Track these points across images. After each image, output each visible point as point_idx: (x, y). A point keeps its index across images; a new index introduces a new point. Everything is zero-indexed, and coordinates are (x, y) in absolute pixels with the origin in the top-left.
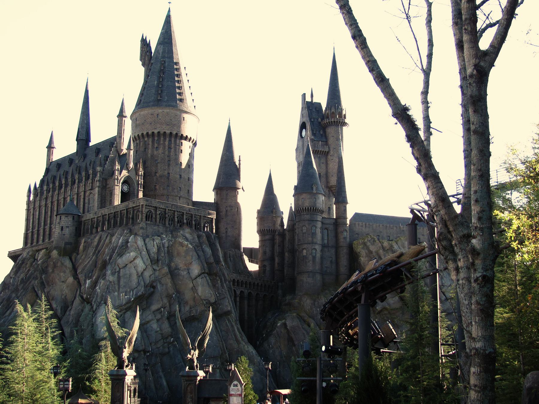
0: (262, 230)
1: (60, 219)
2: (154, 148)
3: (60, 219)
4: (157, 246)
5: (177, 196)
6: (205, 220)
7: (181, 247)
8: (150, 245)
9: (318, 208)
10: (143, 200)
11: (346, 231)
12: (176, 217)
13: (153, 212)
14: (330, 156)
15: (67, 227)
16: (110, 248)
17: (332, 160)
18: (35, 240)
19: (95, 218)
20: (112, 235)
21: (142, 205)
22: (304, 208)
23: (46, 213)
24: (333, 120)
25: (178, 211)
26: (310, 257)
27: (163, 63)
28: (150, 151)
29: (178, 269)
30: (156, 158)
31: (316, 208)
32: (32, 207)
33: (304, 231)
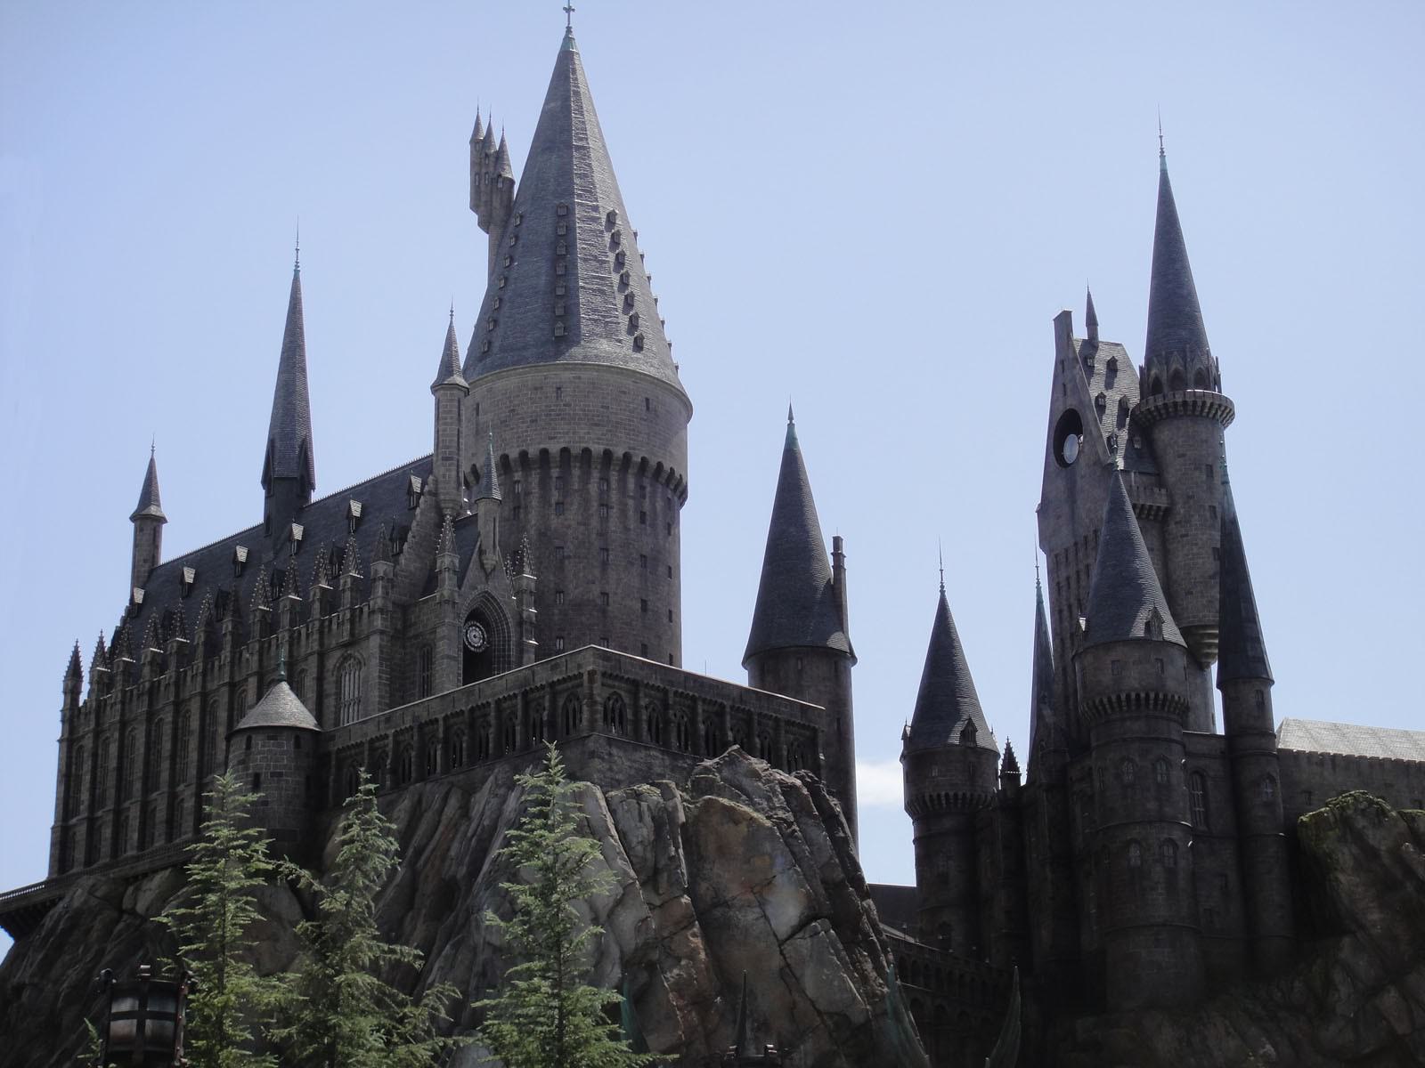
0: (927, 798)
1: (249, 747)
2: (550, 506)
3: (249, 747)
4: (653, 818)
6: (792, 737)
7: (731, 825)
8: (628, 815)
9: (1173, 696)
10: (594, 654)
11: (1273, 780)
12: (700, 719)
13: (627, 701)
14: (1176, 523)
15: (273, 774)
16: (469, 834)
17: (1182, 536)
18: (105, 848)
19: (386, 736)
20: (469, 791)
21: (592, 674)
22: (1123, 697)
23: (152, 745)
24: (1179, 399)
25: (704, 701)
26: (1158, 872)
27: (562, 212)
28: (533, 518)
29: (727, 904)
30: (557, 543)
31: (1165, 696)
32: (87, 727)
33: (1128, 778)
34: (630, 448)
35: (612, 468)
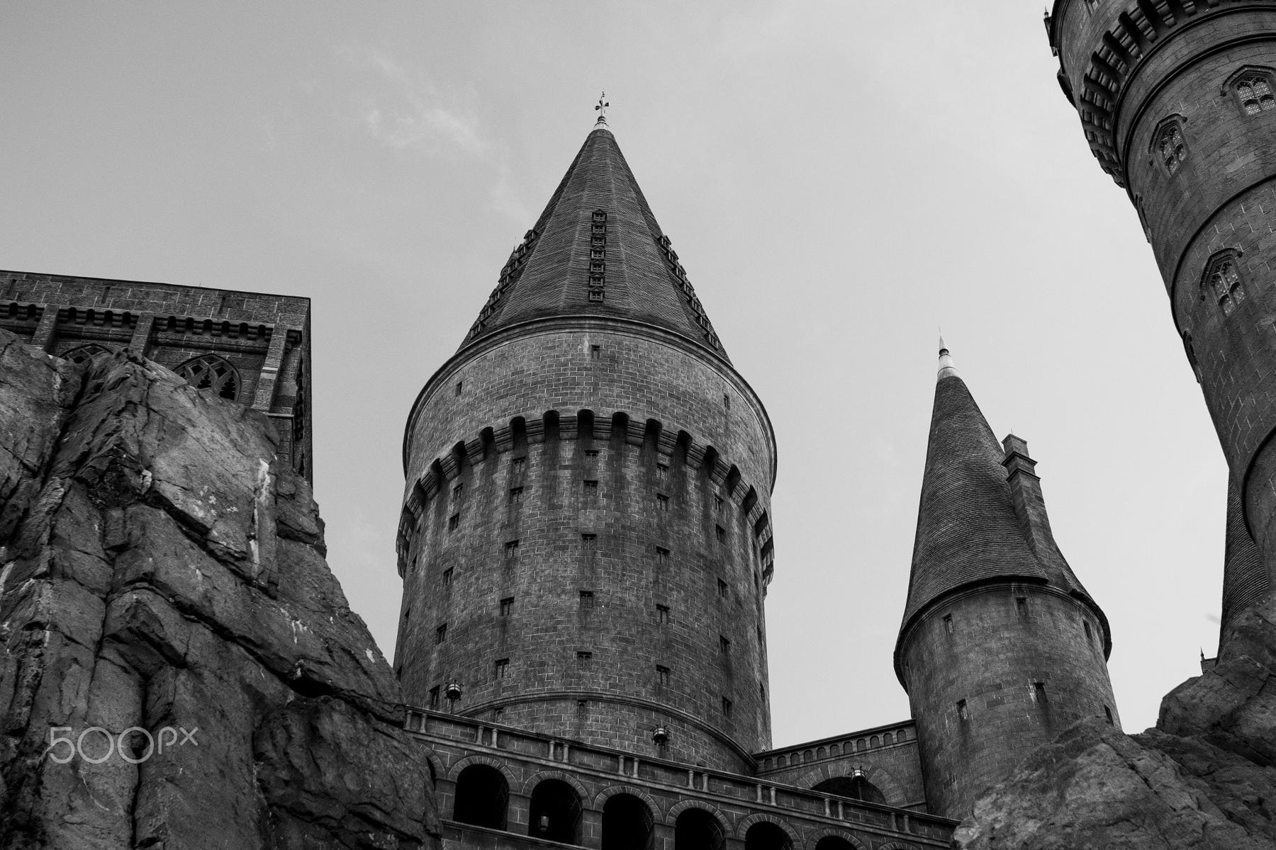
5: (564, 698)
6: (192, 354)
34: (555, 405)
35: (530, 440)
